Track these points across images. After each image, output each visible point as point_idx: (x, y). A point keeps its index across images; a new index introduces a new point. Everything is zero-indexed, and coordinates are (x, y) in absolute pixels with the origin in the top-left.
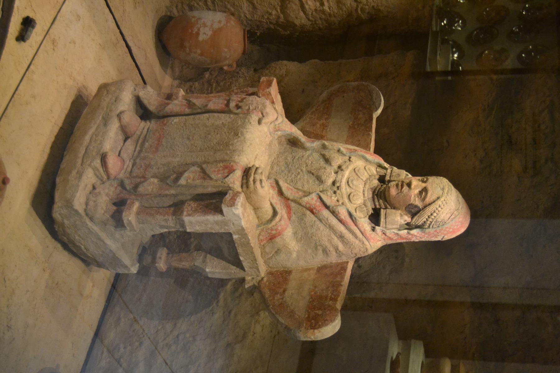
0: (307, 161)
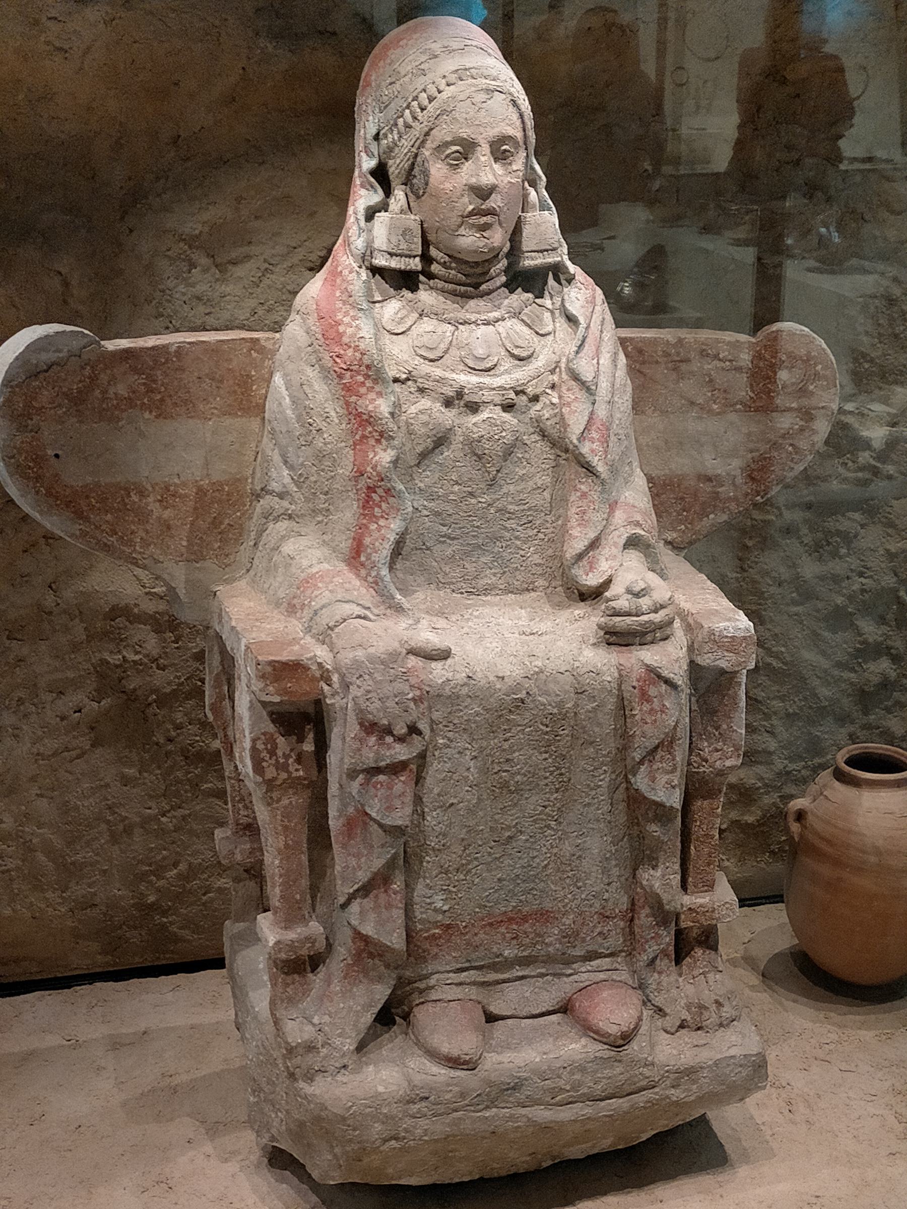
0: (452, 497)
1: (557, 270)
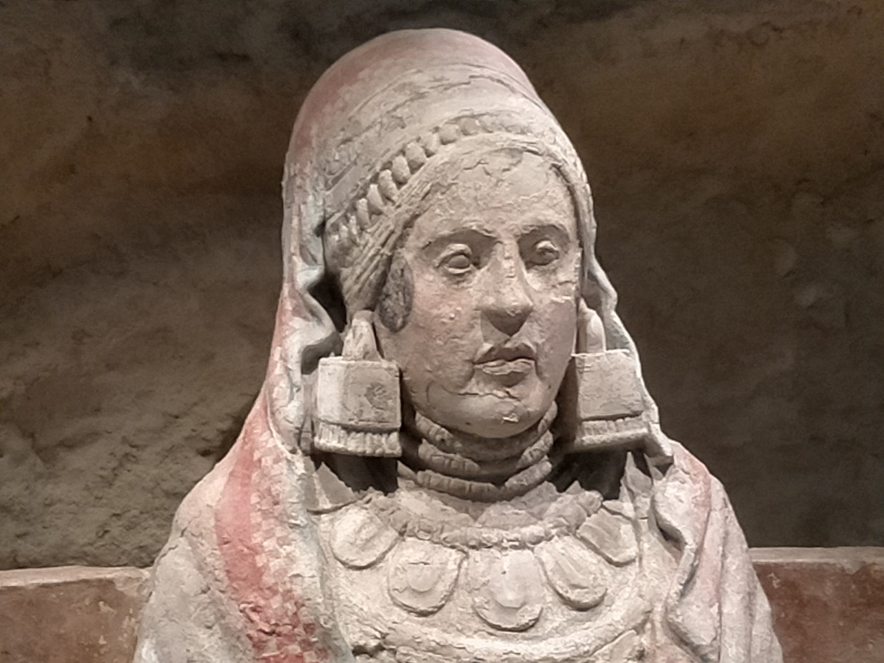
1: (642, 450)
